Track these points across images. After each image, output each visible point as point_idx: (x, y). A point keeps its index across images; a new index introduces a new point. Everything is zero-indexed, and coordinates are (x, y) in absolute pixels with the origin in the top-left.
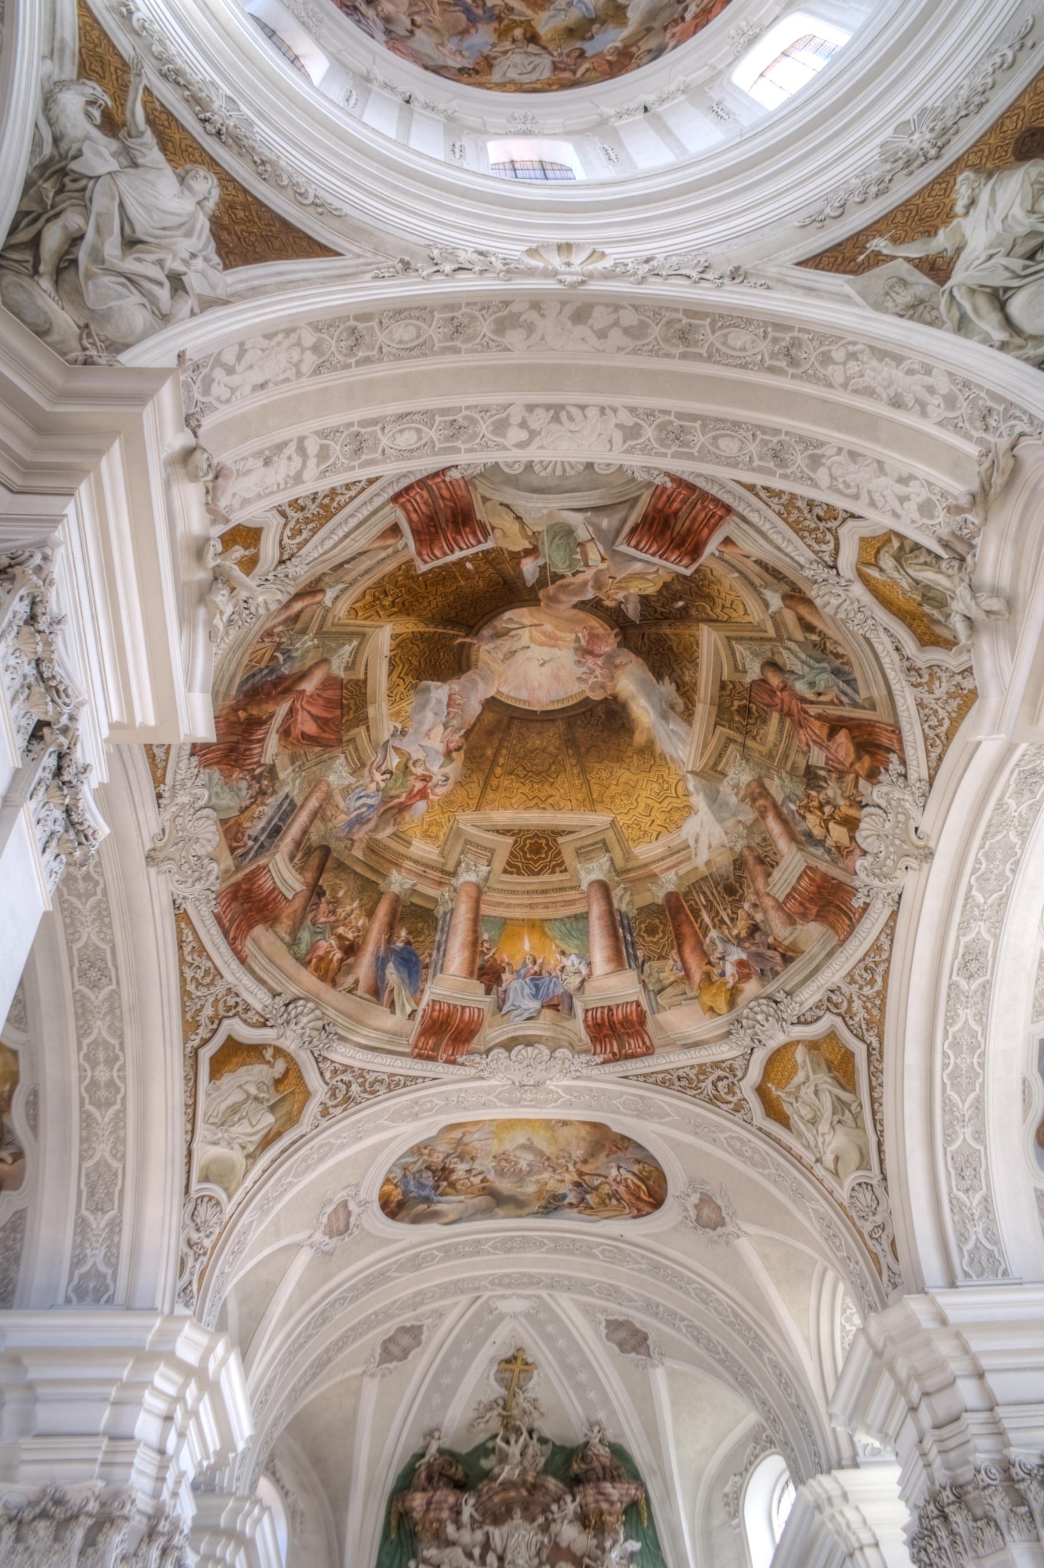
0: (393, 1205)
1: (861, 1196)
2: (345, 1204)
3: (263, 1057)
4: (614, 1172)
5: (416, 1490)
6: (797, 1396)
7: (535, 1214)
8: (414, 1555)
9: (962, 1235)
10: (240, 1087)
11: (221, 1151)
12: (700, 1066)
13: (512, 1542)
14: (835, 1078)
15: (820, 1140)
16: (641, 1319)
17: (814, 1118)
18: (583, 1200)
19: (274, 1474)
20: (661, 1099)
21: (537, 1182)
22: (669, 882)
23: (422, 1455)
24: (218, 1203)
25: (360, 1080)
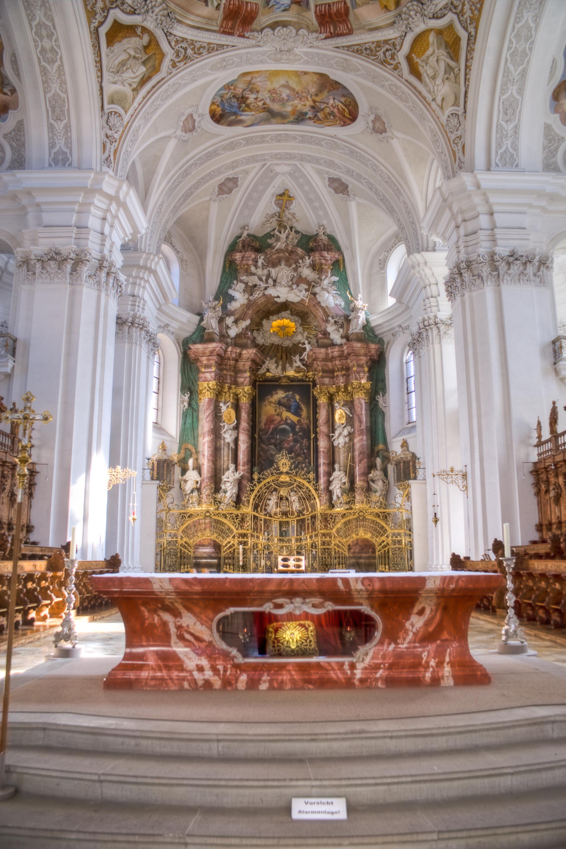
0: (217, 116)
1: (452, 120)
2: (191, 116)
3: (136, 33)
4: (331, 101)
5: (237, 252)
6: (413, 218)
7: (292, 123)
8: (237, 279)
9: (499, 145)
10: (125, 51)
11: (118, 87)
12: (378, 42)
13: (280, 275)
14: (448, 53)
15: (436, 88)
16: (345, 178)
17: (435, 75)
18: (316, 116)
19: (171, 244)
20: (357, 61)
21: (292, 105)
23: (240, 237)
24: (120, 115)
25: (192, 47)
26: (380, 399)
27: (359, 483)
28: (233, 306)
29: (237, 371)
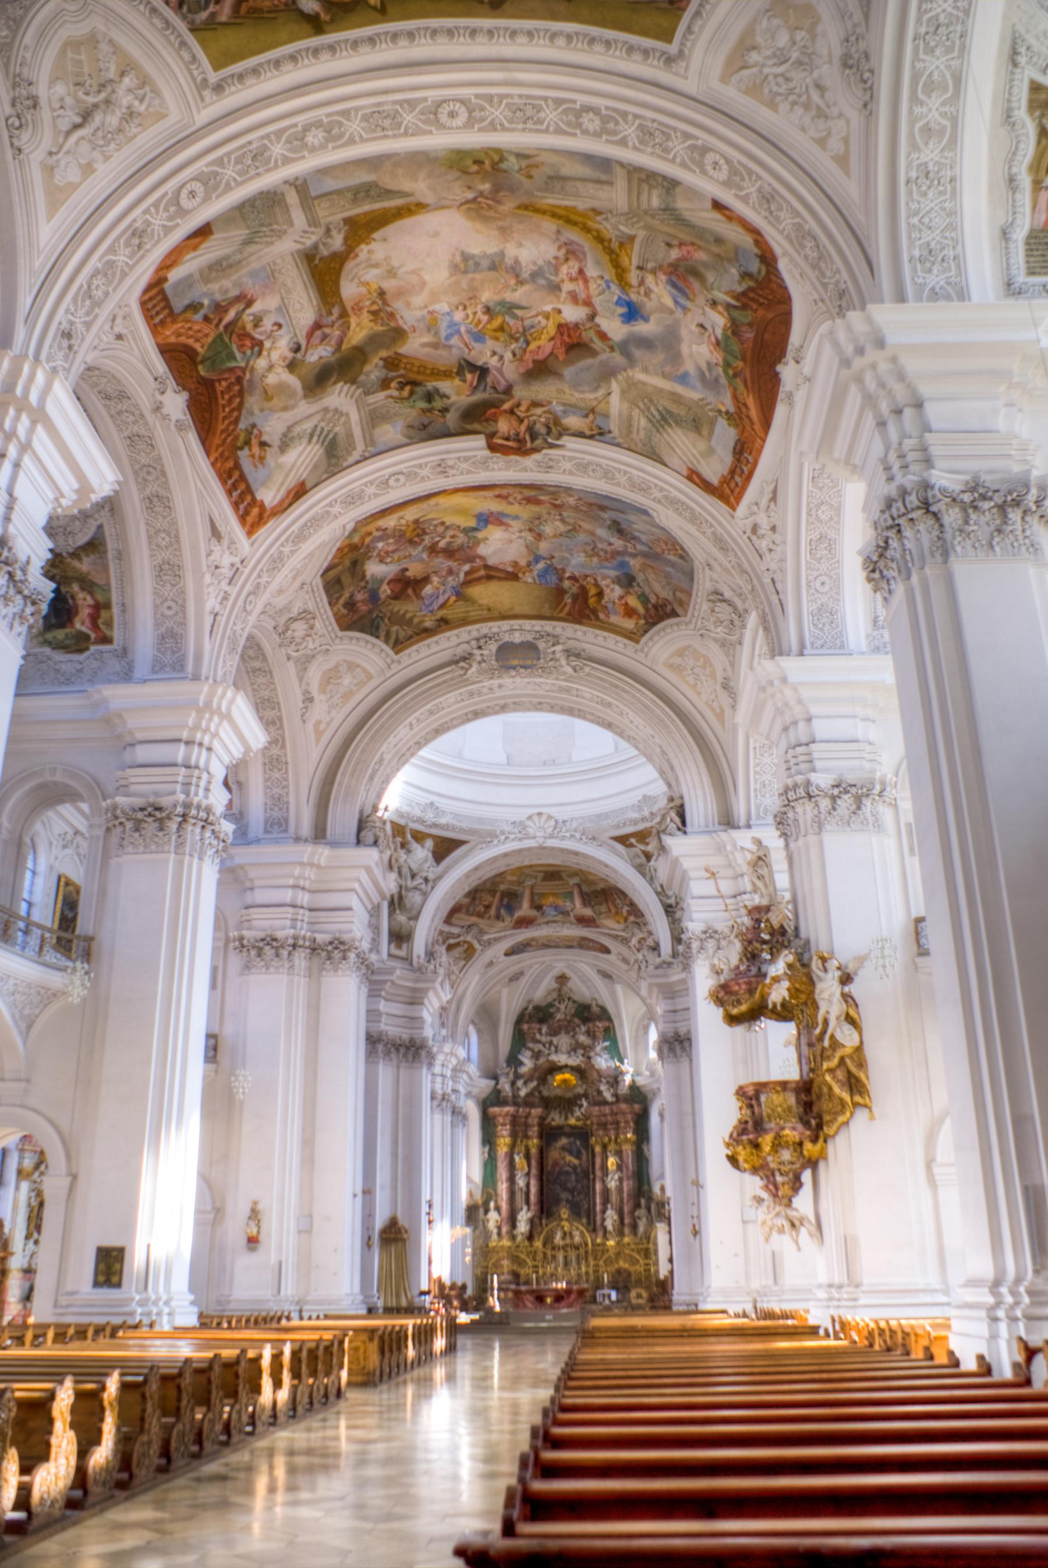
22: (601, 885)
26: (645, 1147)
27: (627, 1221)
28: (523, 1070)
29: (527, 1126)
